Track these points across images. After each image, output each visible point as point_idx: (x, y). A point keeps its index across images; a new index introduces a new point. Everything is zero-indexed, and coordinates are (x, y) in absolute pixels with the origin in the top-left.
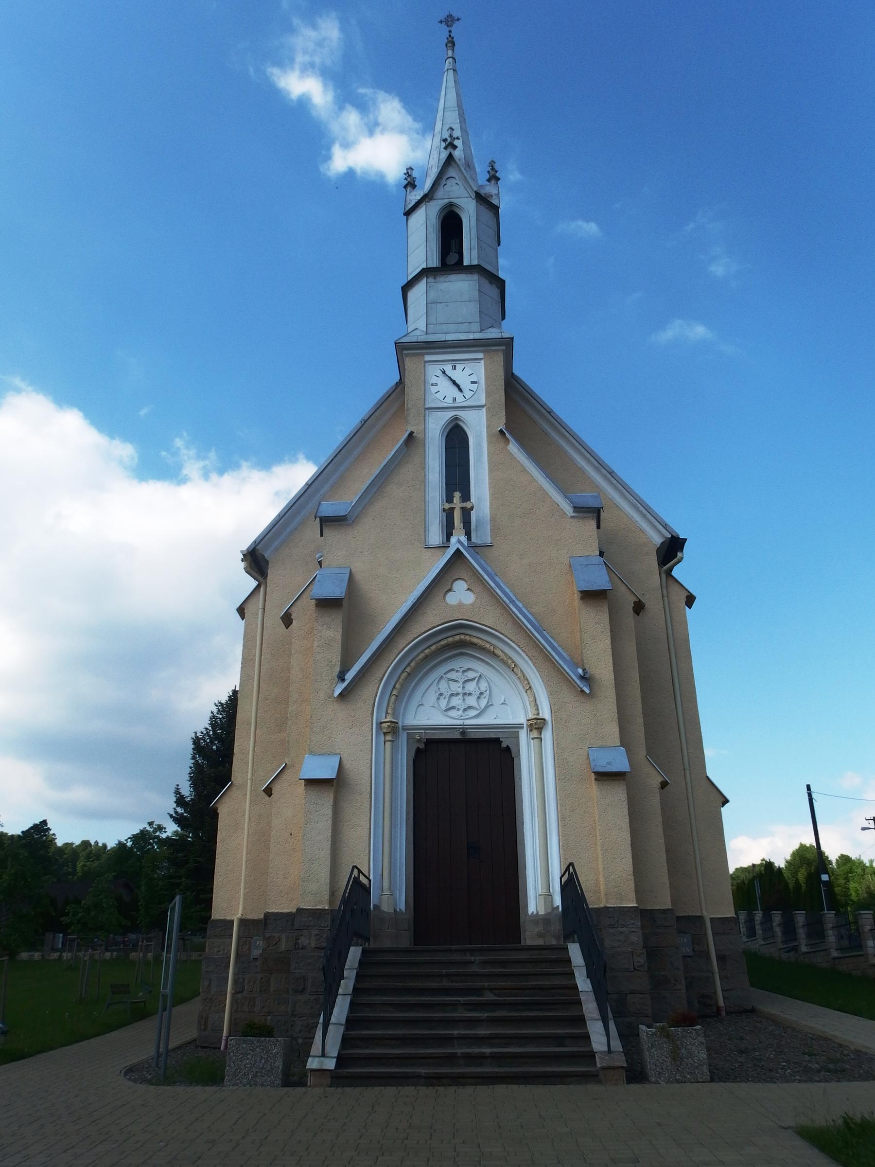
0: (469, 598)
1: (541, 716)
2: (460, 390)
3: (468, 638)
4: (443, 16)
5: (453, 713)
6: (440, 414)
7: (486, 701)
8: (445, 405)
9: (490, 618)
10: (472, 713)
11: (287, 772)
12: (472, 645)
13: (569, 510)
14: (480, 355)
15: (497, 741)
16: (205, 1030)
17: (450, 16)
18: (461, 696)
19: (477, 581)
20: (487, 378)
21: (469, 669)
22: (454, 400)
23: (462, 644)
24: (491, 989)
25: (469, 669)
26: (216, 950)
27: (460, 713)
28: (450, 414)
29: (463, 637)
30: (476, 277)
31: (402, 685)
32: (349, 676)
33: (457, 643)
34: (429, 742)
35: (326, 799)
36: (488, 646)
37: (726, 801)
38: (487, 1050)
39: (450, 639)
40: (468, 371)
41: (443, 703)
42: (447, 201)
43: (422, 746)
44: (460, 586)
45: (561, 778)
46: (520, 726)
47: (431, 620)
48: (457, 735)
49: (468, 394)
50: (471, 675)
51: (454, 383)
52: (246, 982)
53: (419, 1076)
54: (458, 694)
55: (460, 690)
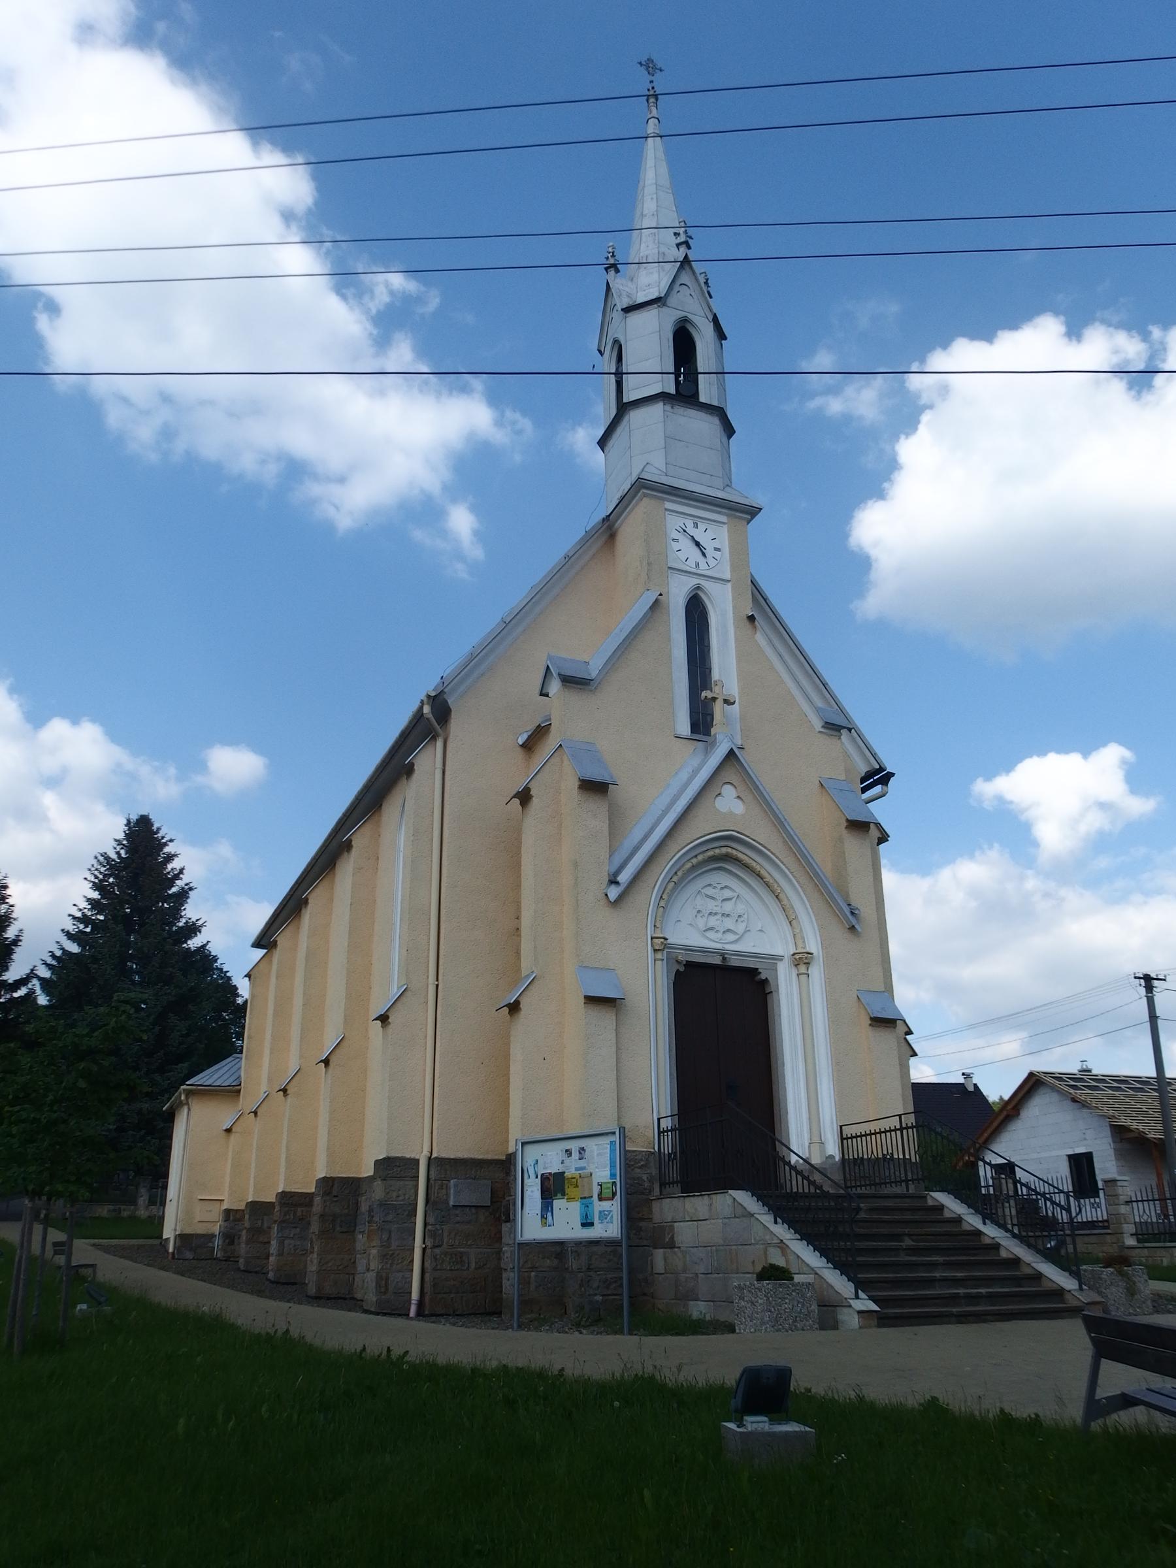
0: (739, 808)
1: (808, 950)
2: (704, 555)
3: (734, 852)
4: (643, 60)
5: (710, 934)
6: (683, 578)
7: (744, 925)
8: (688, 569)
9: (760, 832)
10: (731, 937)
11: (536, 982)
12: (736, 860)
13: (818, 725)
14: (724, 519)
15: (754, 972)
16: (385, 1293)
17: (650, 60)
18: (719, 917)
19: (752, 788)
20: (731, 547)
21: (726, 887)
22: (697, 564)
23: (727, 858)
24: (910, 1235)
25: (726, 887)
26: (395, 1194)
27: (719, 935)
28: (693, 581)
29: (729, 850)
30: (661, 404)
31: (670, 896)
32: (624, 878)
33: (724, 855)
34: (689, 965)
35: (606, 1018)
36: (754, 864)
37: (914, 1054)
38: (961, 1291)
39: (717, 851)
40: (711, 534)
41: (701, 923)
42: (684, 314)
43: (682, 969)
44: (728, 791)
45: (834, 1019)
46: (780, 958)
47: (701, 827)
48: (717, 960)
49: (712, 563)
50: (727, 894)
51: (698, 544)
52: (445, 1234)
53: (951, 1315)
54: (716, 914)
55: (716, 909)
